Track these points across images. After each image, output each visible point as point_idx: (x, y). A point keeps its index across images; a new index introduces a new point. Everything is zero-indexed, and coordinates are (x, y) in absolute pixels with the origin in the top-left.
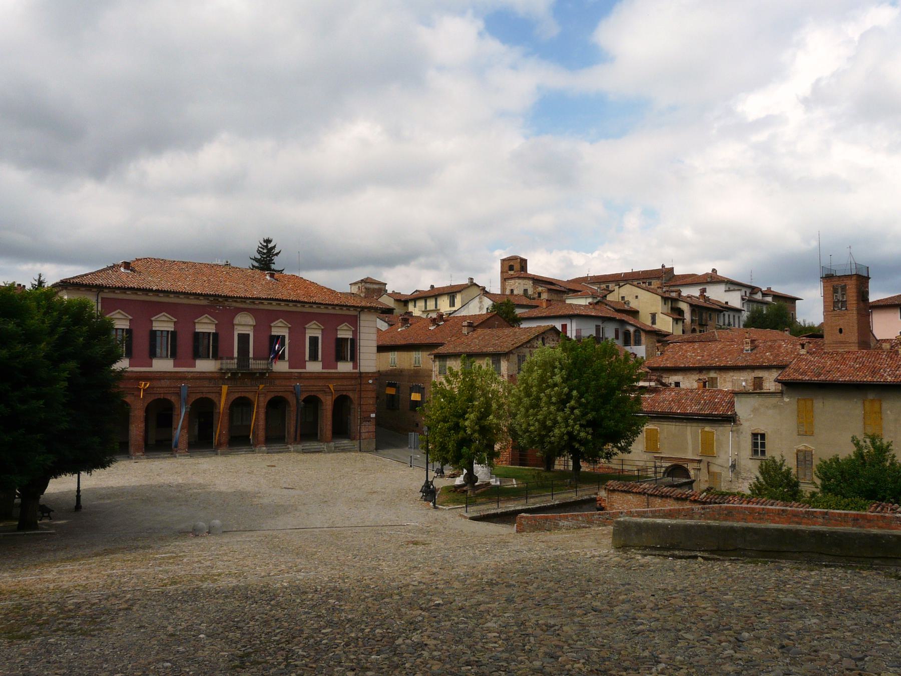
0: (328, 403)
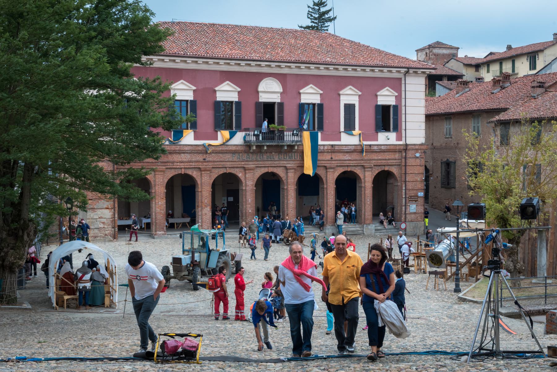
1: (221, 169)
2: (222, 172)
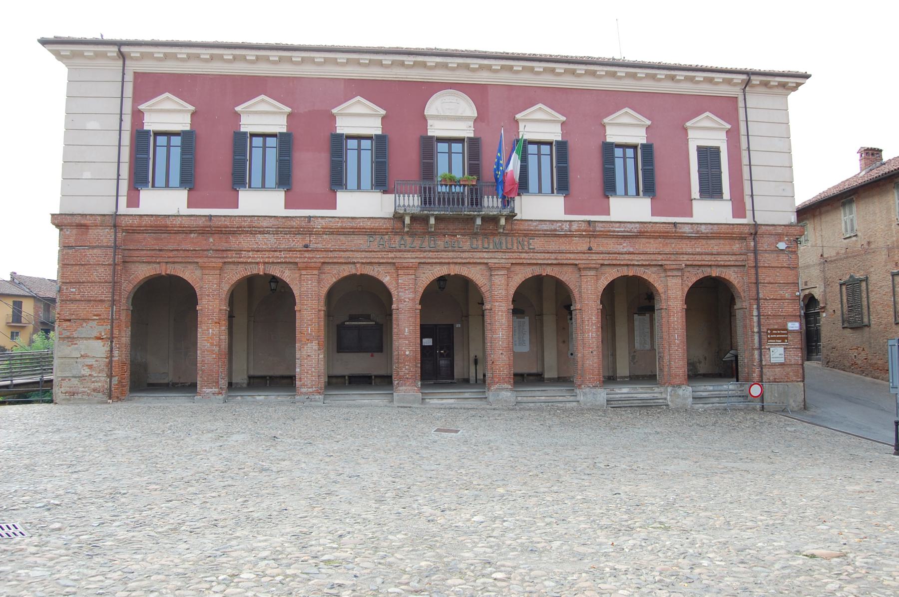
0: (672, 294)
1: (345, 267)
2: (346, 274)
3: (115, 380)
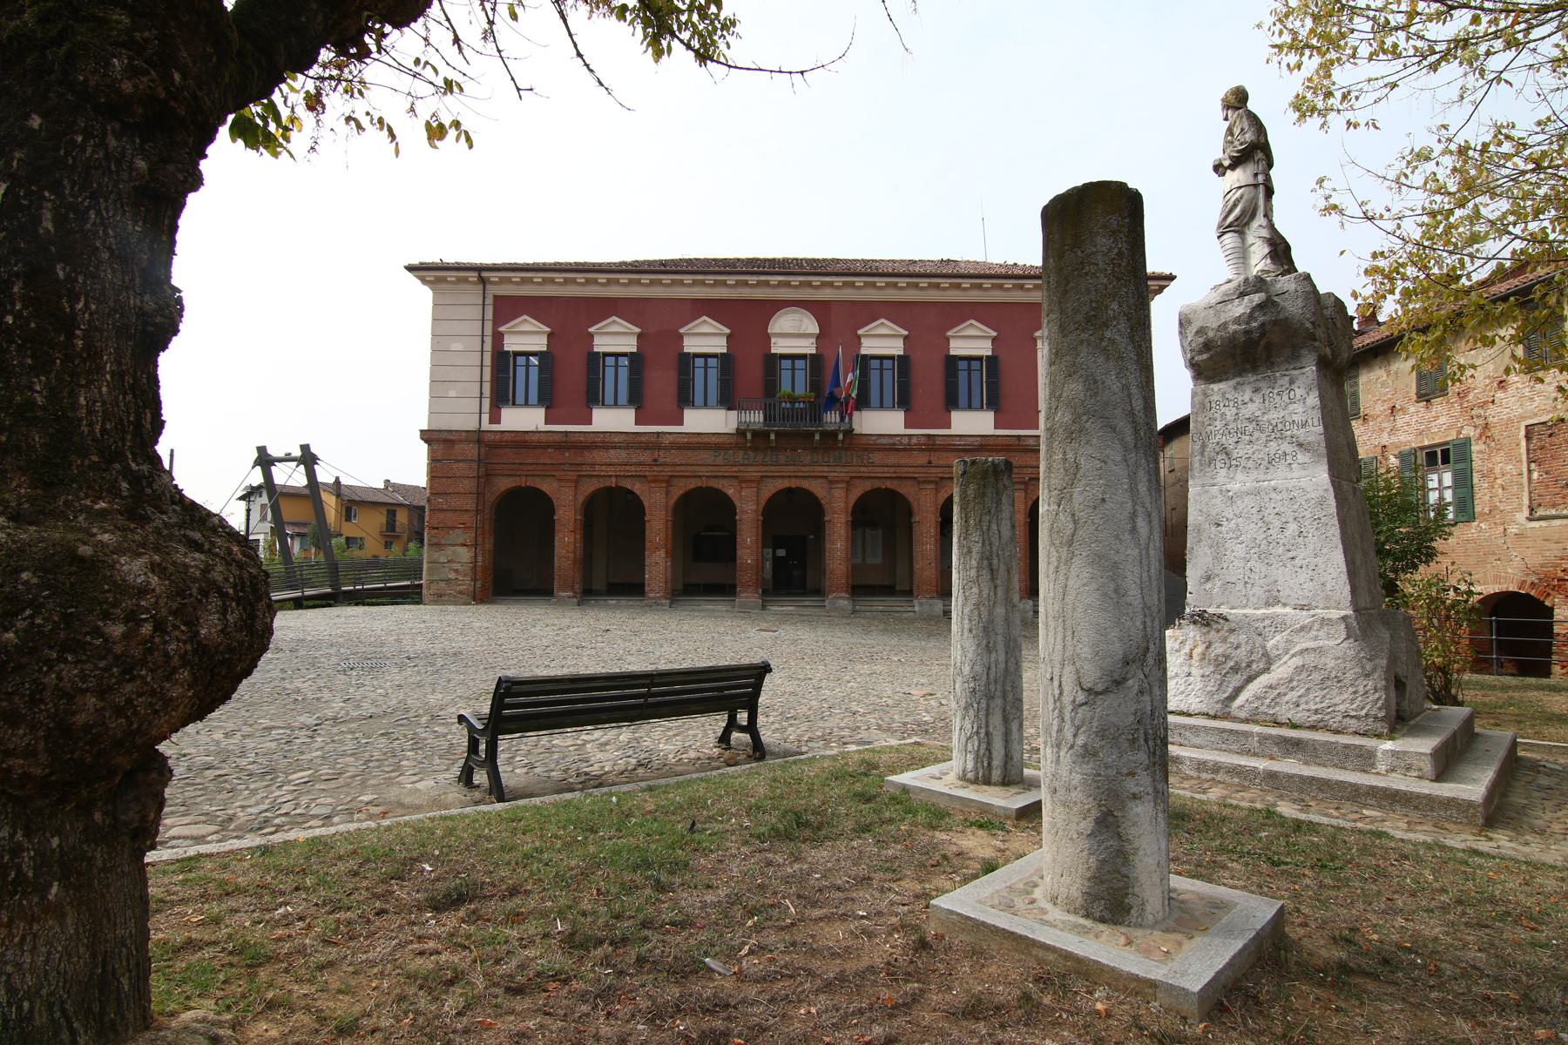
3: (479, 584)
